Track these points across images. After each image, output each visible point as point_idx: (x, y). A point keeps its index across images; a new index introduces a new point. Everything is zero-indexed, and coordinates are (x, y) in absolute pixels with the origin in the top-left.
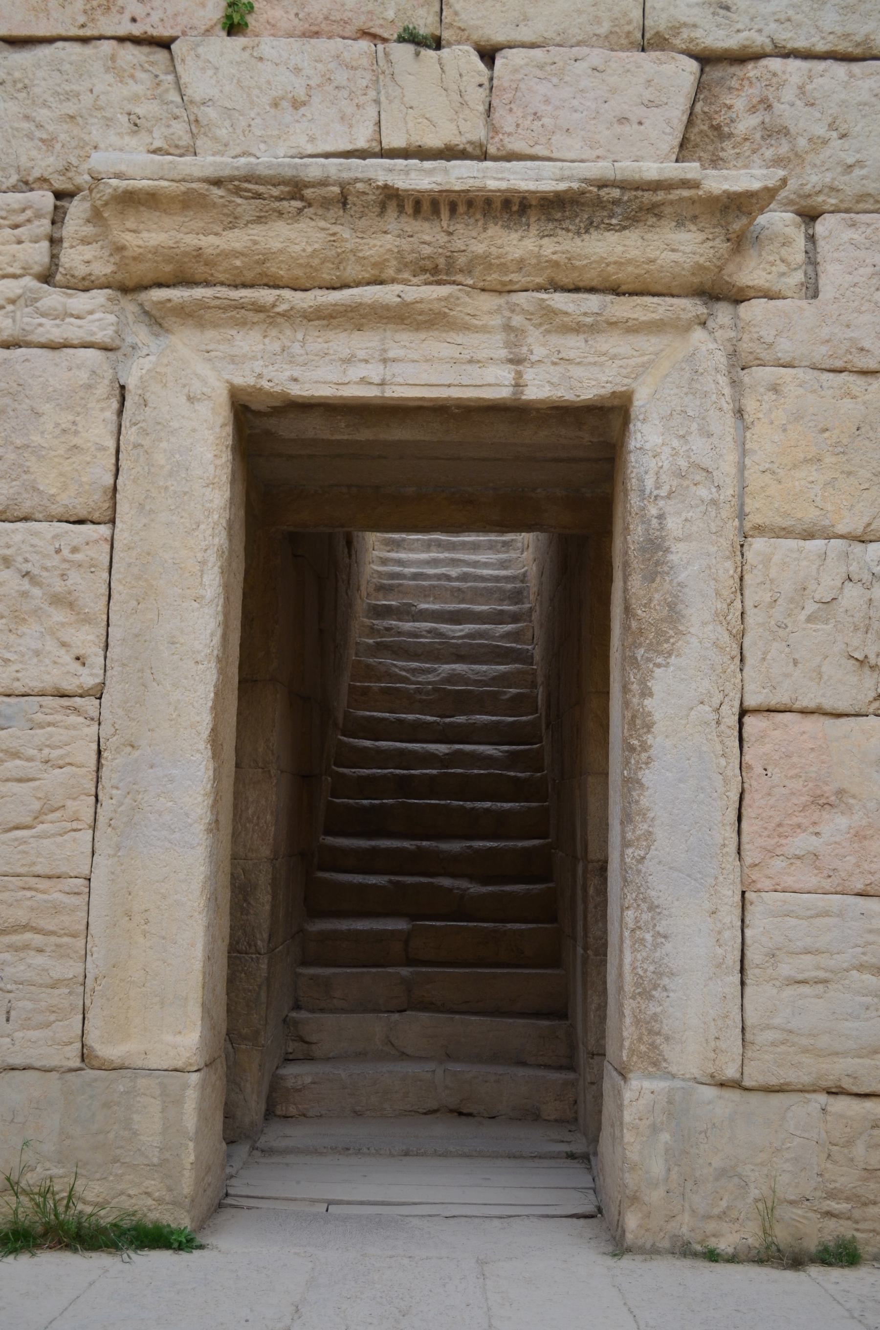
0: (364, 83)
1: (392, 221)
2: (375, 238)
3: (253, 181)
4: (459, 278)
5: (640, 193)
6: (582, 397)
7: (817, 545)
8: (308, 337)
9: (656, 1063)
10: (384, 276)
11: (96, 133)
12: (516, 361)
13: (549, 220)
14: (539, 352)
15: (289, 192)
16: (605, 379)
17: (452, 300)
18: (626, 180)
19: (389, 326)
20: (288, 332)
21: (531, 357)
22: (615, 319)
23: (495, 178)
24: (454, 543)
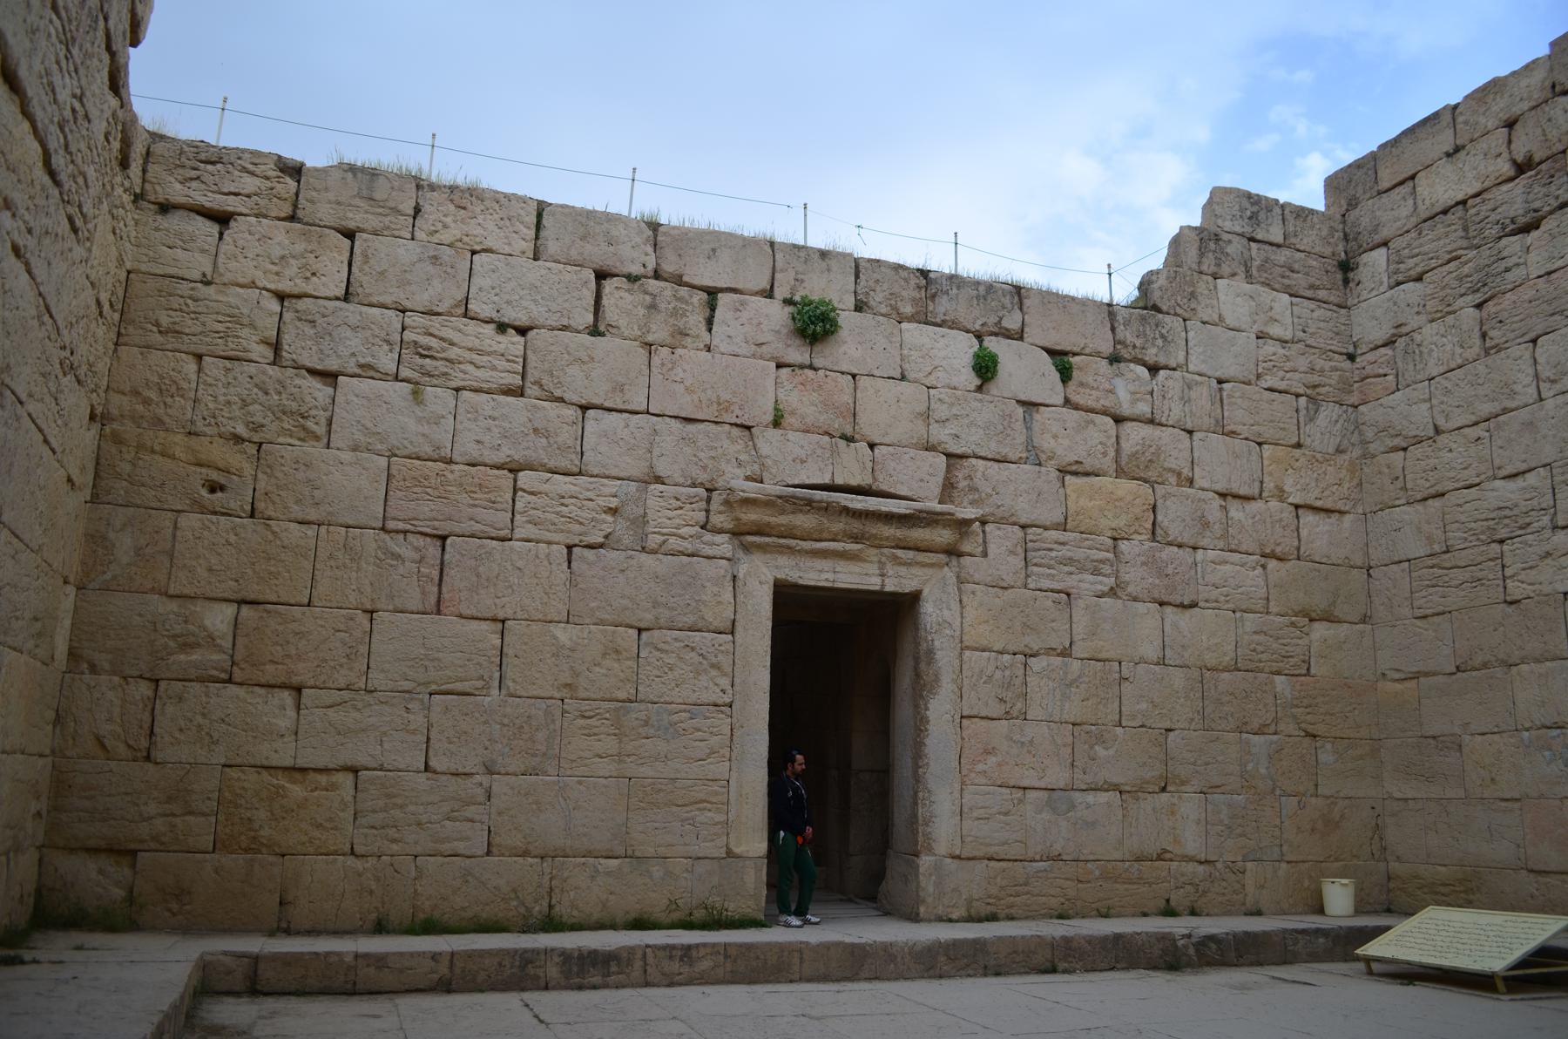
1: (843, 519)
7: (986, 654)
9: (930, 850)
11: (723, 466)
12: (882, 575)
14: (891, 573)
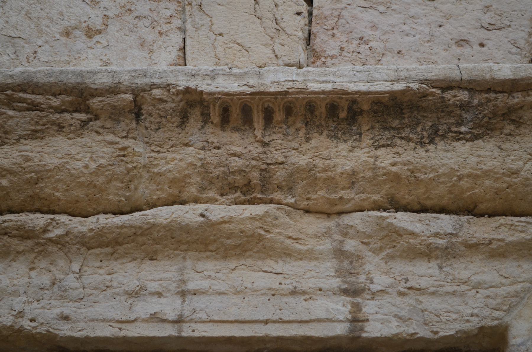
0: (169, 13)
1: (194, 132)
2: (175, 152)
3: (29, 91)
4: (277, 195)
5: (492, 95)
6: (442, 334)
8: (85, 268)
10: (185, 196)
12: (352, 292)
13: (385, 128)
14: (381, 281)
15: (71, 103)
16: (469, 311)
17: (269, 220)
18: (475, 81)
19: (190, 253)
20: (62, 263)
21: (371, 286)
22: (475, 240)
23: (317, 81)
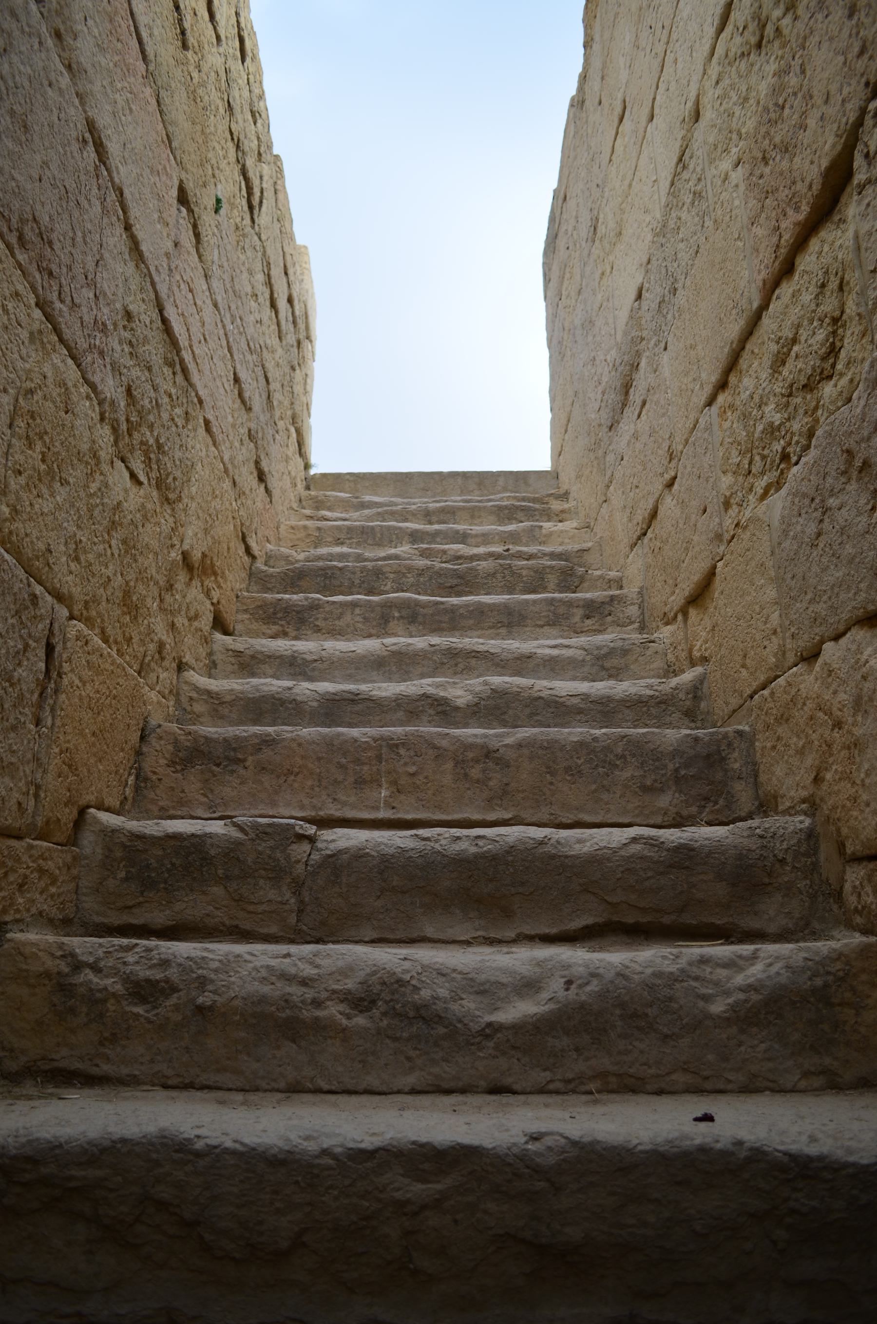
24: (453, 610)
